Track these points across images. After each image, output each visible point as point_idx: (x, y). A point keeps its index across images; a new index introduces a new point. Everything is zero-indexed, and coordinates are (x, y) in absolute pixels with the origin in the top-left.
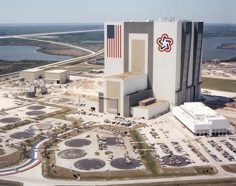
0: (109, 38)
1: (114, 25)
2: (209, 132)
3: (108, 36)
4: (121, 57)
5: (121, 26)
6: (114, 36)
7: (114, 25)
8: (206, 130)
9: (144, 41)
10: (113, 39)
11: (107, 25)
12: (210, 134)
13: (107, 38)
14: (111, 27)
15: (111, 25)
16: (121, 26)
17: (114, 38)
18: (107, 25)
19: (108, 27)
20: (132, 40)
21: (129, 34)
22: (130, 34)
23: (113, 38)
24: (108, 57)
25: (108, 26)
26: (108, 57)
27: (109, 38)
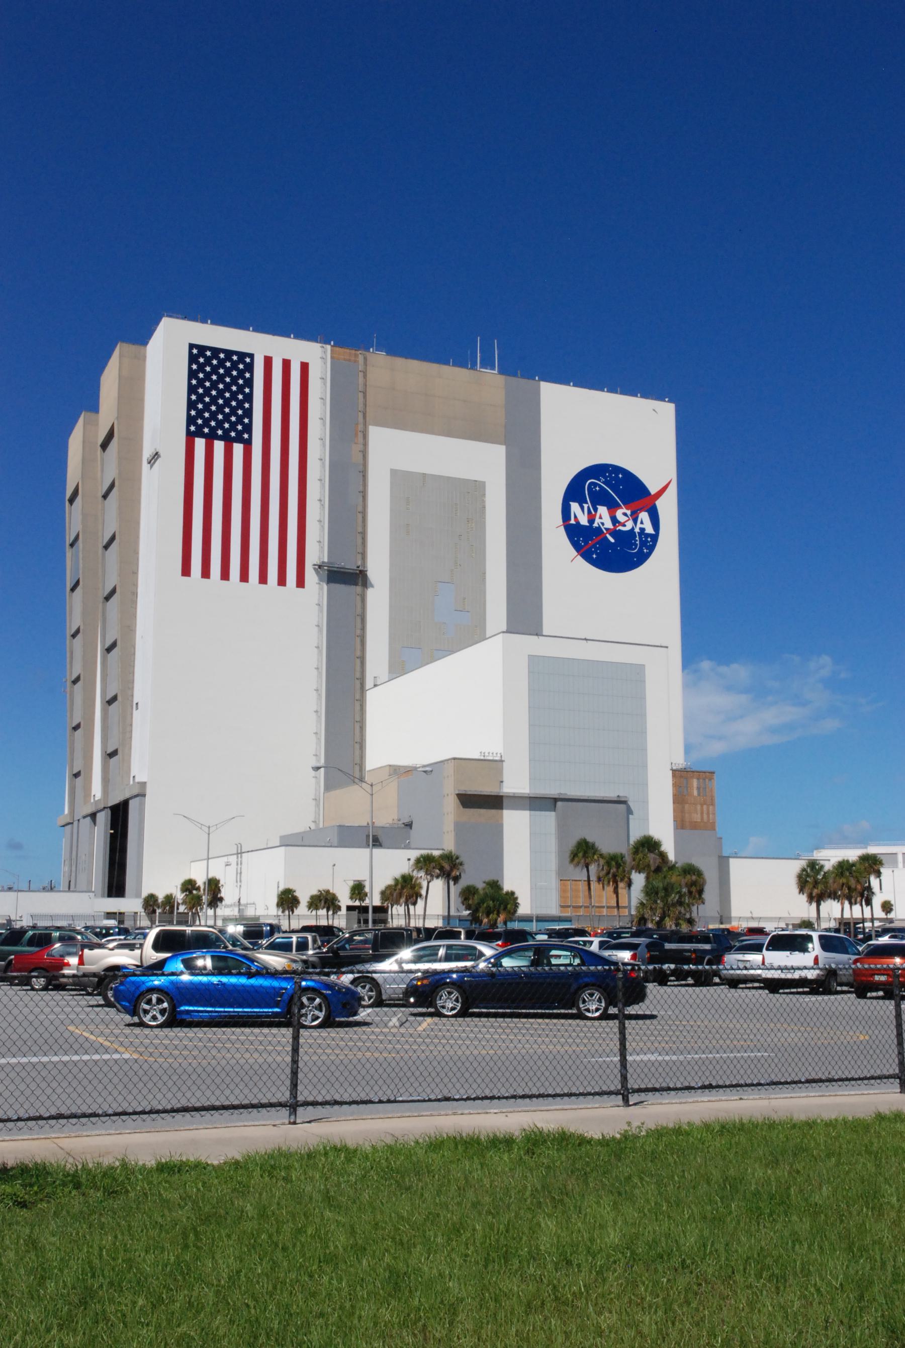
1: (251, 356)
3: (190, 420)
4: (301, 583)
5: (305, 367)
6: (248, 428)
7: (251, 356)
11: (192, 346)
14: (221, 363)
15: (229, 353)
16: (305, 367)
17: (248, 444)
18: (192, 346)
19: (192, 359)
23: (239, 439)
24: (186, 571)
25: (198, 355)
26: (186, 571)
27: (199, 433)
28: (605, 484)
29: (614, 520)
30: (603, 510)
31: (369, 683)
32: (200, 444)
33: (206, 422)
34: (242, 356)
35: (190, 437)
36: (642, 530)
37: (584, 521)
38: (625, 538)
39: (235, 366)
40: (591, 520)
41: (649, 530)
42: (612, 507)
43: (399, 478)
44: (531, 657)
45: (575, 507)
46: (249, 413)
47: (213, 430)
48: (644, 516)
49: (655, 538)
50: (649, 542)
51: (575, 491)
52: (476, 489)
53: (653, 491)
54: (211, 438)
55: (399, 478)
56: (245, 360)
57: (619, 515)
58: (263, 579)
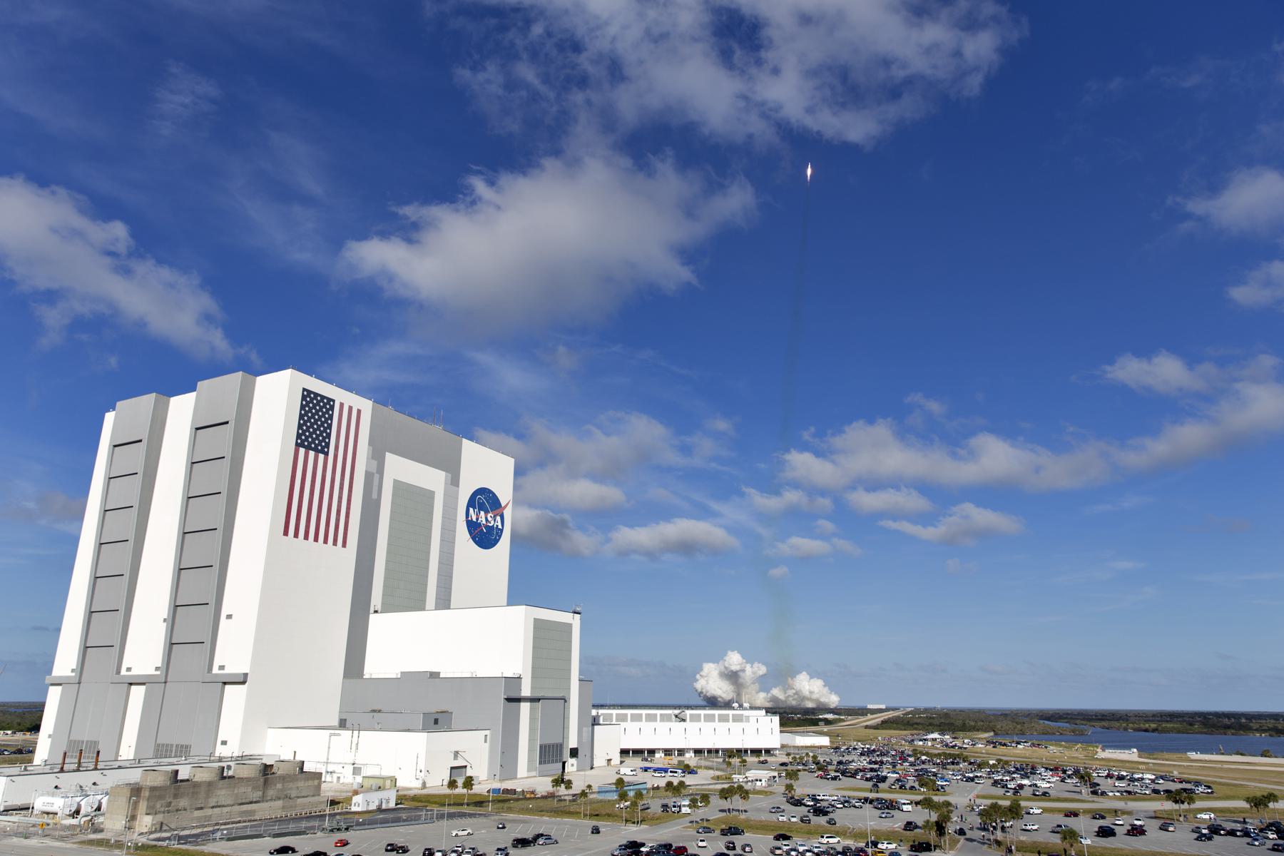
0: (303, 446)
3: (299, 436)
4: (344, 545)
5: (359, 411)
6: (328, 445)
9: (431, 495)
10: (321, 456)
11: (304, 390)
13: (297, 445)
14: (318, 402)
15: (323, 397)
16: (359, 411)
17: (327, 454)
18: (304, 390)
19: (304, 398)
21: (388, 454)
22: (390, 458)
24: (286, 533)
26: (286, 533)
28: (484, 499)
30: (482, 513)
31: (372, 610)
32: (302, 451)
33: (306, 440)
34: (330, 400)
39: (325, 406)
42: (487, 512)
43: (398, 485)
44: (535, 620)
47: (310, 444)
48: (498, 518)
51: (471, 503)
52: (431, 495)
54: (308, 448)
55: (398, 485)
58: (326, 541)
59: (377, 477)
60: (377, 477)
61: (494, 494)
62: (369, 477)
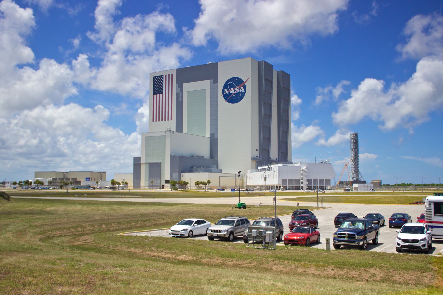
2: (302, 183)
3: (154, 92)
4: (171, 119)
5: (172, 75)
6: (163, 90)
8: (297, 181)
10: (161, 95)
12: (305, 185)
15: (159, 76)
16: (172, 75)
17: (162, 93)
19: (154, 80)
20: (189, 93)
24: (153, 121)
26: (153, 121)
29: (235, 91)
30: (232, 89)
35: (154, 94)
36: (242, 91)
37: (227, 93)
38: (237, 94)
40: (229, 92)
41: (243, 91)
42: (234, 87)
45: (226, 90)
46: (163, 87)
48: (242, 88)
49: (245, 93)
50: (243, 94)
51: (225, 86)
53: (244, 81)
54: (157, 94)
55: (189, 93)
56: (162, 76)
57: (236, 89)
59: (181, 93)
60: (181, 93)
61: (238, 78)
62: (178, 95)
